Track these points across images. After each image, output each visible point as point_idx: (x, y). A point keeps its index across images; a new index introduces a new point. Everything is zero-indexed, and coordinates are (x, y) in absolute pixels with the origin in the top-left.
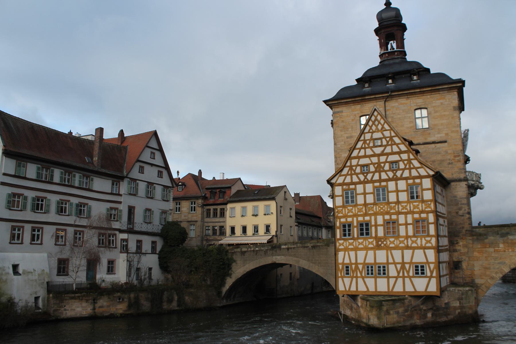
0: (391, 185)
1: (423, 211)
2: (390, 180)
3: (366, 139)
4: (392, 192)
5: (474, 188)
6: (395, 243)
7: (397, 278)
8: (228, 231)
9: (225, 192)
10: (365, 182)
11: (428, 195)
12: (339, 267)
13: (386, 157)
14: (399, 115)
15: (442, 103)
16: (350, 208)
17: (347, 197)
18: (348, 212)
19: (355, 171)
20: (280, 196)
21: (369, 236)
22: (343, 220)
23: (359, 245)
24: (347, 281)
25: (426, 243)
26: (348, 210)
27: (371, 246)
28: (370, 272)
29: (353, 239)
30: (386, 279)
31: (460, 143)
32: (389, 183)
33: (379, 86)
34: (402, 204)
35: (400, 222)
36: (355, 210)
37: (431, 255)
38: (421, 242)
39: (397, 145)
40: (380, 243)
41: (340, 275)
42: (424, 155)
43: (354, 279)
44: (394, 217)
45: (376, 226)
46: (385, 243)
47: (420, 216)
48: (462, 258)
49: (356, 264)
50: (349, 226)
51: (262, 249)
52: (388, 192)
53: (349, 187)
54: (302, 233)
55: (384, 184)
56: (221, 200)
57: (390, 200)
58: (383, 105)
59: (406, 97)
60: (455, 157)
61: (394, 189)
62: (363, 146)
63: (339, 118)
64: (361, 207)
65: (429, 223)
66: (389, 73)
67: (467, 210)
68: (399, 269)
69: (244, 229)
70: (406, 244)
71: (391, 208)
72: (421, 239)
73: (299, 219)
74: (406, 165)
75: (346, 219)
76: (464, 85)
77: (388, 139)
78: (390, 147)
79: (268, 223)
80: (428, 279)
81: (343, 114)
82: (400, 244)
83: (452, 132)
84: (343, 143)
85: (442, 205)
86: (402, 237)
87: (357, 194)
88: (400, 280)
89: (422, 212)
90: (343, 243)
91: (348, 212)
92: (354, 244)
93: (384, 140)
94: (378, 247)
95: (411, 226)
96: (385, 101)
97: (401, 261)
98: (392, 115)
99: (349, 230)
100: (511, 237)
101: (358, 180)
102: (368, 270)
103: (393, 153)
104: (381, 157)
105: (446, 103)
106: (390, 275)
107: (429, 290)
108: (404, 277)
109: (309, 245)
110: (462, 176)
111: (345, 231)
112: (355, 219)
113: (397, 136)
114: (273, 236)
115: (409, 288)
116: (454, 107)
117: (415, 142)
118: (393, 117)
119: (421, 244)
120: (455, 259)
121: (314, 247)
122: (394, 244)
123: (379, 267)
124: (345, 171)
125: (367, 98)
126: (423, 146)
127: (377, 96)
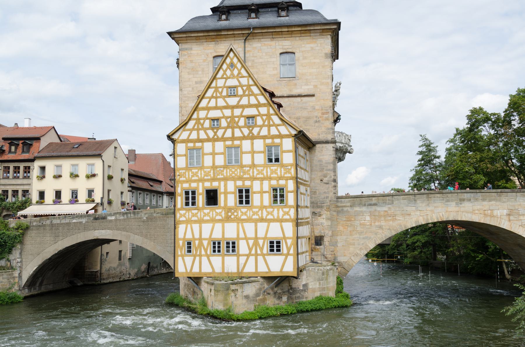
0: (246, 145)
2: (244, 138)
3: (218, 86)
4: (246, 153)
5: (341, 153)
6: (248, 214)
7: (248, 256)
8: (35, 197)
9: (31, 145)
10: (214, 140)
11: (288, 158)
12: (179, 244)
13: (241, 109)
15: (312, 48)
16: (195, 171)
18: (192, 176)
19: (202, 125)
20: (108, 154)
22: (186, 186)
23: (204, 216)
24: (189, 260)
27: (218, 217)
28: (217, 249)
29: (198, 209)
30: (235, 258)
31: (330, 97)
32: (243, 141)
33: (238, 20)
34: (258, 168)
36: (201, 174)
37: (289, 229)
38: (278, 213)
39: (255, 96)
40: (230, 214)
41: (179, 253)
42: (287, 109)
44: (248, 183)
45: (226, 193)
46: (235, 214)
47: (278, 183)
48: (324, 233)
49: (201, 239)
50: (194, 193)
52: (242, 153)
54: (137, 200)
55: (237, 143)
56: (26, 156)
59: (271, 37)
60: (323, 114)
61: (249, 149)
62: (214, 95)
64: (209, 170)
66: (253, 5)
67: (333, 177)
68: (251, 246)
69: (58, 194)
70: (260, 215)
71: (245, 173)
72: (278, 211)
73: (133, 183)
74: (264, 121)
75: (190, 185)
76: (339, 29)
78: (247, 98)
79: (90, 187)
80: (284, 257)
81: (193, 52)
82: (253, 215)
84: (190, 89)
85: (305, 170)
87: (204, 154)
88: (252, 259)
89: (280, 178)
90: (185, 214)
91: (192, 176)
92: (199, 215)
94: (228, 219)
95: (267, 194)
96: (245, 40)
97: (253, 236)
98: (253, 58)
99: (194, 198)
100: (378, 209)
102: (214, 247)
103: (250, 106)
106: (240, 253)
108: (256, 255)
110: (329, 137)
111: (187, 198)
113: (256, 85)
114: (98, 203)
115: (262, 269)
116: (326, 54)
117: (276, 94)
118: (253, 61)
120: (317, 233)
123: (228, 243)
126: (287, 99)
127: (235, 32)
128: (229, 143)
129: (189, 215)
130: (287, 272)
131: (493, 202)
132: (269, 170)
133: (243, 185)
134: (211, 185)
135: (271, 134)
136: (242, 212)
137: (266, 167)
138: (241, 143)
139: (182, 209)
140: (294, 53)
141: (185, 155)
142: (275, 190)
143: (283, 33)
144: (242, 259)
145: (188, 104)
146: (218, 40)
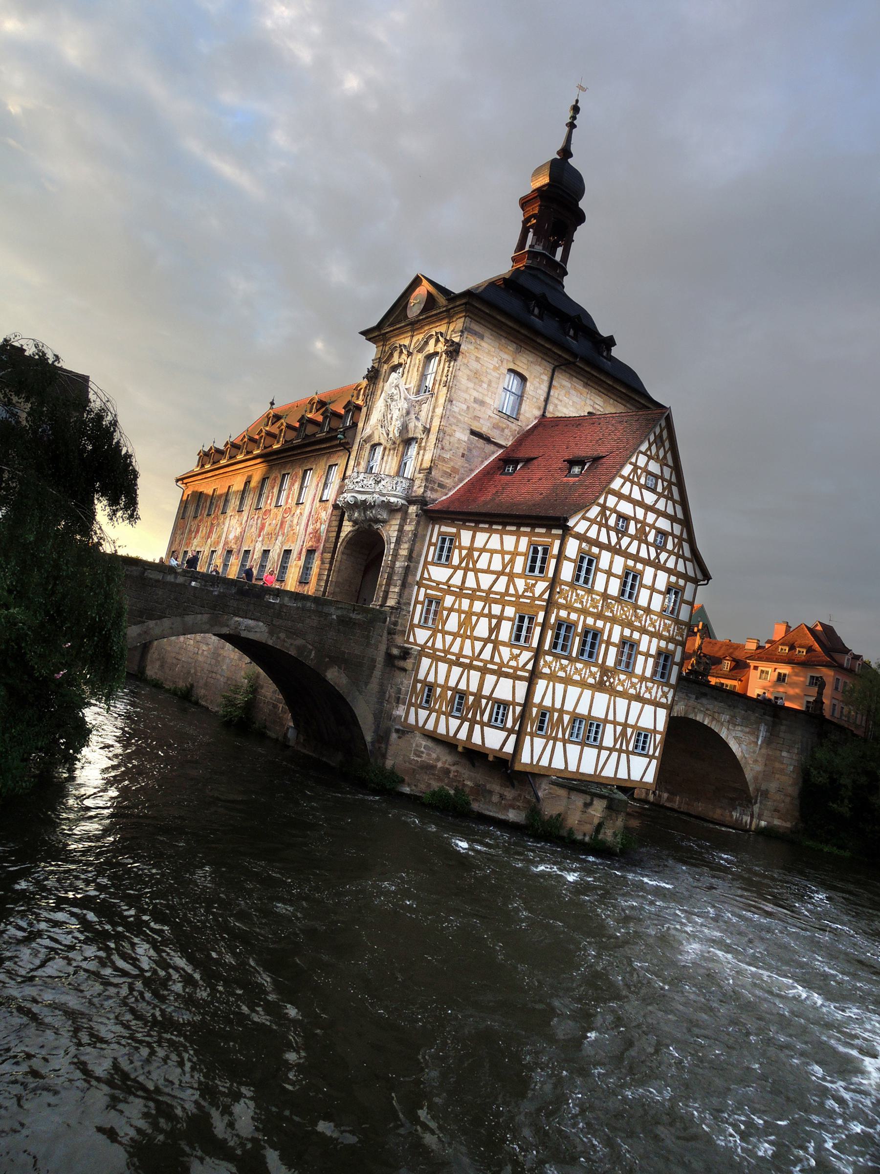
2: (647, 562)
4: (646, 587)
13: (655, 516)
14: (565, 406)
16: (581, 593)
17: (580, 569)
19: (607, 520)
21: (593, 660)
22: (563, 614)
24: (539, 742)
26: (577, 595)
27: (591, 681)
30: (596, 751)
32: (647, 567)
34: (652, 616)
38: (657, 693)
40: (605, 678)
41: (529, 730)
43: (551, 742)
44: (636, 635)
45: (609, 643)
46: (612, 680)
49: (561, 711)
50: (569, 628)
55: (639, 566)
58: (550, 374)
62: (631, 477)
63: (472, 347)
64: (598, 598)
75: (569, 614)
81: (483, 344)
84: (464, 407)
86: (636, 676)
88: (615, 755)
92: (568, 669)
93: (660, 481)
94: (600, 686)
97: (623, 721)
98: (556, 402)
104: (649, 513)
107: (645, 780)
108: (620, 751)
111: (557, 636)
112: (582, 617)
115: (622, 774)
118: (556, 406)
119: (656, 697)
122: (623, 685)
125: (539, 340)
129: (555, 665)
130: (647, 783)
133: (631, 636)
134: (595, 624)
135: (678, 569)
136: (619, 680)
137: (661, 618)
139: (549, 653)
141: (574, 561)
143: (605, 386)
144: (604, 754)
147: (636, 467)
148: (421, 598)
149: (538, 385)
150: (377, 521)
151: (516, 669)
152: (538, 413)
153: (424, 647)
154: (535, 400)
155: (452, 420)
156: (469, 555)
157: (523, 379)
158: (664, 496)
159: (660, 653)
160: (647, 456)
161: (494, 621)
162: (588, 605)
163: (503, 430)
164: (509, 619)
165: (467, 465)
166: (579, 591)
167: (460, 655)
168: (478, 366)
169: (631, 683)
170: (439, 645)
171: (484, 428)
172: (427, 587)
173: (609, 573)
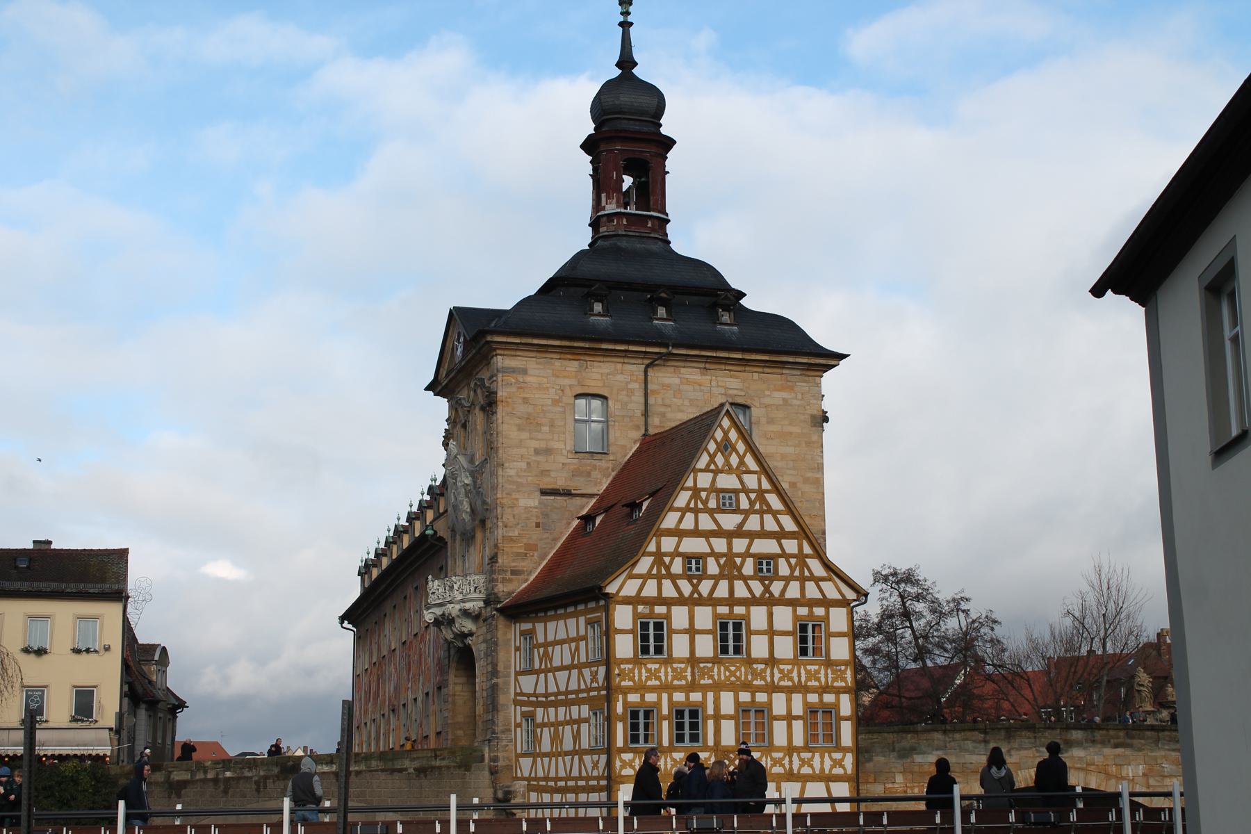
0: (758, 617)
1: (827, 686)
2: (753, 601)
4: (758, 633)
18: (648, 678)
19: (668, 568)
22: (633, 698)
25: (832, 767)
26: (649, 670)
32: (753, 609)
34: (782, 667)
35: (776, 712)
36: (666, 674)
38: (822, 763)
39: (775, 514)
44: (761, 697)
45: (718, 717)
50: (647, 714)
51: (247, 773)
52: (750, 632)
53: (652, 610)
55: (740, 610)
57: (754, 655)
59: (702, 365)
61: (764, 626)
62: (692, 505)
63: (514, 389)
64: (683, 666)
65: (840, 718)
70: (787, 766)
71: (756, 674)
72: (822, 757)
74: (792, 569)
75: (642, 697)
77: (753, 496)
79: (84, 680)
81: (528, 379)
83: (806, 480)
84: (523, 465)
86: (779, 749)
87: (672, 631)
91: (648, 678)
93: (742, 496)
96: (647, 366)
98: (662, 409)
101: (675, 595)
103: (764, 534)
105: (796, 402)
109: (407, 763)
111: (635, 727)
112: (665, 696)
116: (813, 417)
118: (663, 415)
119: (822, 769)
121: (422, 771)
124: (644, 565)
125: (604, 346)
127: (632, 348)
128: (723, 610)
131: (1120, 751)
132: (803, 671)
134: (688, 697)
138: (748, 612)
139: (625, 750)
140: (745, 407)
141: (632, 631)
142: (814, 712)
145: (517, 499)
146: (587, 358)
147: (696, 491)
148: (518, 720)
149: (626, 399)
150: (464, 636)
151: (598, 778)
152: (637, 435)
153: (529, 779)
154: (627, 419)
155: (507, 486)
156: (546, 653)
157: (604, 398)
158: (756, 512)
159: (811, 711)
160: (711, 471)
161: (575, 726)
162: (670, 678)
163: (589, 474)
164: (587, 720)
165: (546, 535)
166: (649, 666)
167: (557, 779)
168: (530, 409)
169: (772, 759)
170: (540, 774)
171: (561, 483)
172: (522, 704)
173: (692, 631)
